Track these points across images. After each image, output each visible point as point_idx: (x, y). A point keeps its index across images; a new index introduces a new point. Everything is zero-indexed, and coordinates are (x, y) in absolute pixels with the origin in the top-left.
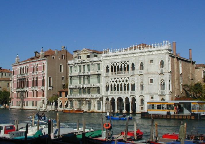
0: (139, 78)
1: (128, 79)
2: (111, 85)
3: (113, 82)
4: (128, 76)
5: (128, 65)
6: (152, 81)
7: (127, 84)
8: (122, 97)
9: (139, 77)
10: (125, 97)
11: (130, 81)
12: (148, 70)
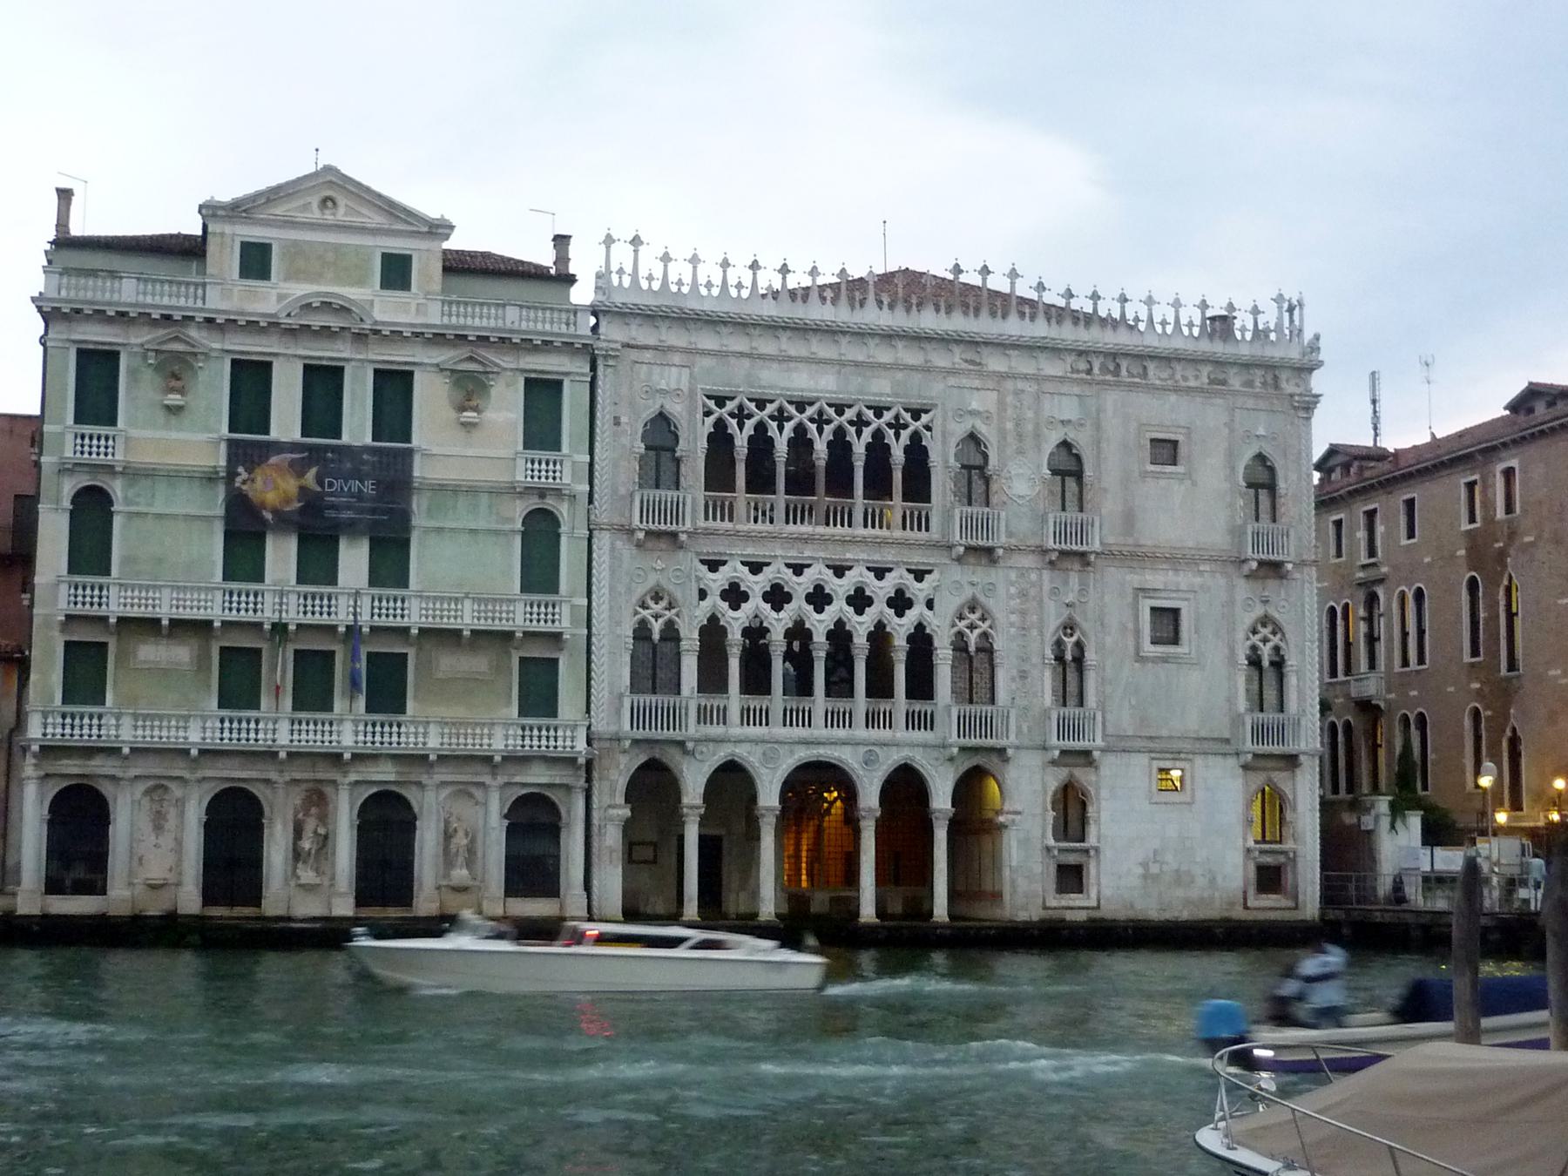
0: (1047, 586)
1: (918, 590)
2: (713, 632)
3: (734, 595)
4: (918, 559)
5: (917, 453)
6: (1168, 623)
7: (901, 629)
8: (848, 758)
9: (1046, 574)
10: (890, 760)
11: (949, 604)
12: (1129, 520)
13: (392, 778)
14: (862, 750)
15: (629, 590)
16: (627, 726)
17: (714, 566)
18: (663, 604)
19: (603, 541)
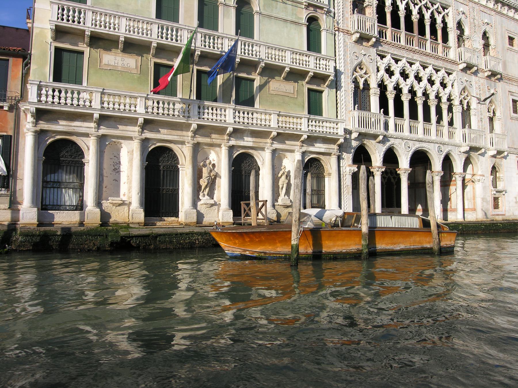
3: (390, 72)
13: (250, 144)
14: (437, 145)
15: (352, 61)
16: (357, 126)
17: (382, 57)
18: (364, 71)
19: (340, 36)
